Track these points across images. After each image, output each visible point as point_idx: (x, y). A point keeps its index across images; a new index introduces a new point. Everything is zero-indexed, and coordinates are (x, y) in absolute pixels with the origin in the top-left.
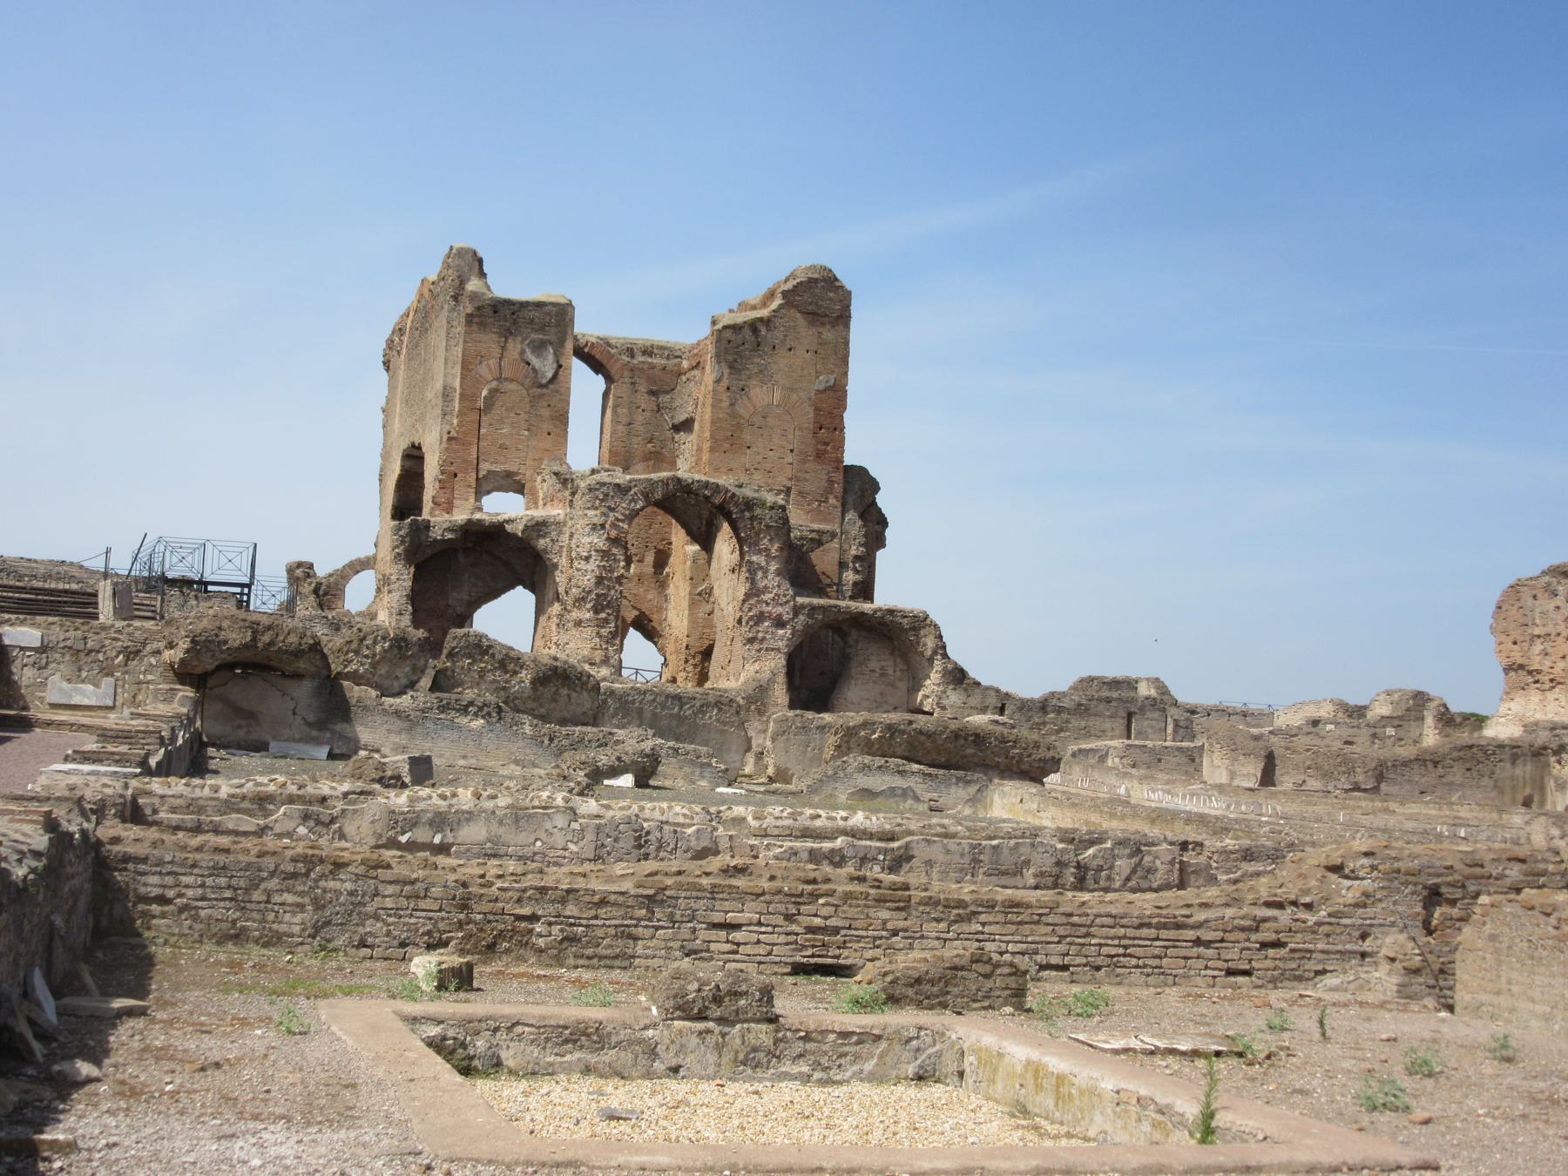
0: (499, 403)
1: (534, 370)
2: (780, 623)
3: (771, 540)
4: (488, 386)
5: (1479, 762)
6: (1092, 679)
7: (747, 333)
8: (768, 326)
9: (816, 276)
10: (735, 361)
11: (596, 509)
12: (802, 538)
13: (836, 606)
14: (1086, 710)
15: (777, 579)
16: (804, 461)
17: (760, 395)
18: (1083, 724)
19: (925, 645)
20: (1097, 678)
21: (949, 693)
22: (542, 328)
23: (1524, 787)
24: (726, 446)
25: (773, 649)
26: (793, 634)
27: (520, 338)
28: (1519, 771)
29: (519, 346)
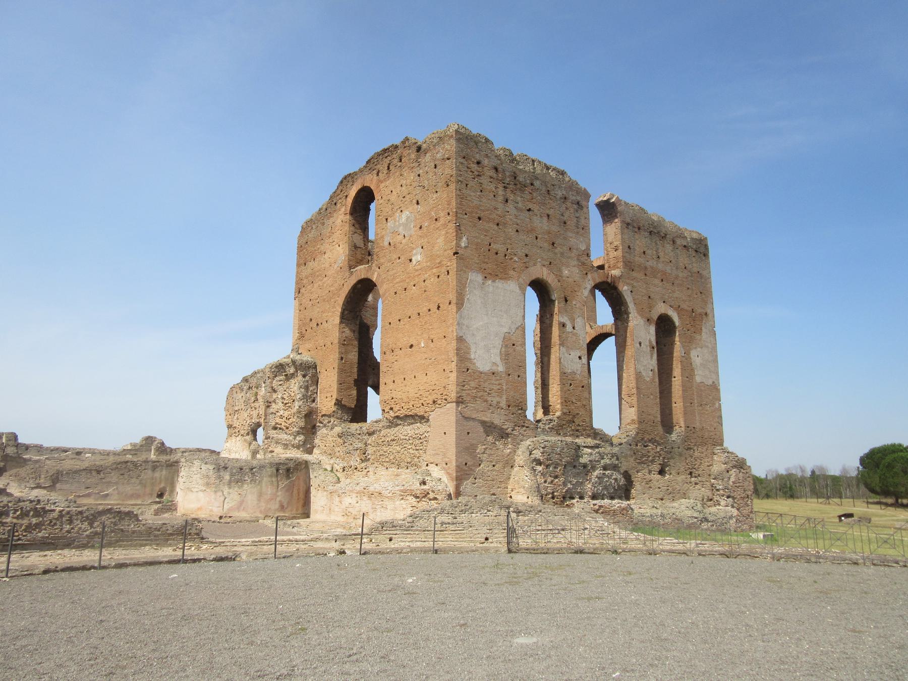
5: (129, 471)
23: (160, 482)
28: (157, 474)
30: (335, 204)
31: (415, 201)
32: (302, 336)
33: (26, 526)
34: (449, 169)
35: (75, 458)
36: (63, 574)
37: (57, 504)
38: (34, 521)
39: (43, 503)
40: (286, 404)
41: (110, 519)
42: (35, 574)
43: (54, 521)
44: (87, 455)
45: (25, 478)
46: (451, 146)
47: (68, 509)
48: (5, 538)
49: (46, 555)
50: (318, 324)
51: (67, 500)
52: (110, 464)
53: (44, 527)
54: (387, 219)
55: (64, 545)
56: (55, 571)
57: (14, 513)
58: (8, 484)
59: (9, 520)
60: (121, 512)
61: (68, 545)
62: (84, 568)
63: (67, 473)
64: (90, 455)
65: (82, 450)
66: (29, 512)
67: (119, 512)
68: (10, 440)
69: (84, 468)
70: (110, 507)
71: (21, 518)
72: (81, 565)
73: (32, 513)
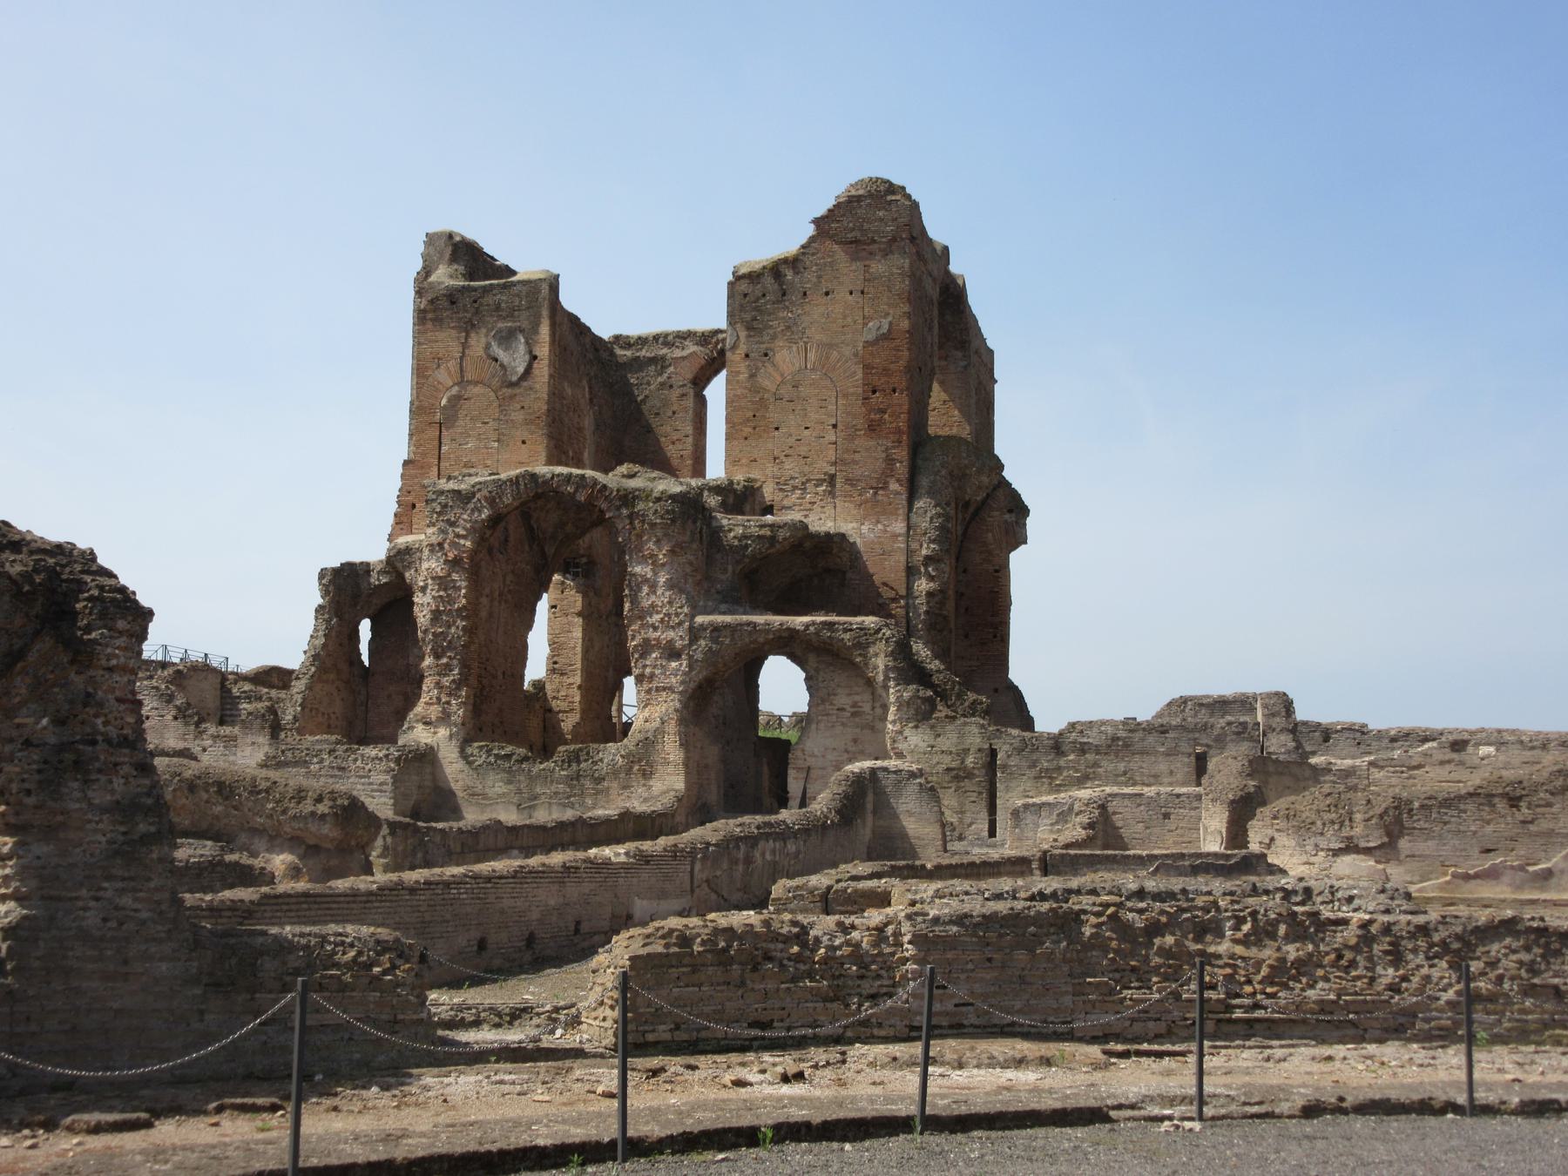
0: (462, 413)
1: (502, 366)
2: (673, 653)
3: (658, 541)
4: (448, 394)
6: (1184, 701)
7: (768, 281)
8: (794, 268)
9: (861, 192)
10: (755, 319)
11: (434, 525)
12: (745, 537)
13: (749, 624)
14: (1126, 746)
15: (668, 593)
16: (851, 438)
17: (787, 358)
18: (1121, 766)
19: (875, 667)
20: (1191, 698)
21: (907, 732)
22: (511, 314)
24: (747, 430)
25: (664, 689)
26: (690, 666)
27: (484, 331)
29: (483, 340)
33: (1271, 966)
35: (1449, 762)
36: (1359, 1124)
37: (1356, 902)
38: (1292, 951)
39: (1319, 899)
41: (1514, 952)
42: (1280, 1117)
43: (1348, 955)
44: (1485, 750)
45: (1312, 823)
47: (1386, 918)
48: (1218, 1000)
49: (1330, 1058)
51: (1383, 891)
52: (1545, 774)
53: (1320, 972)
55: (1386, 1030)
56: (1339, 1109)
57: (1237, 928)
58: (1272, 839)
59: (1223, 947)
60: (1546, 929)
61: (1399, 1027)
62: (1425, 1107)
63: (1422, 806)
64: (1491, 749)
65: (1466, 736)
66: (1274, 924)
67: (1543, 931)
68: (1273, 715)
69: (1471, 790)
70: (1509, 913)
71: (1255, 945)
72: (1416, 1097)
73: (1282, 929)
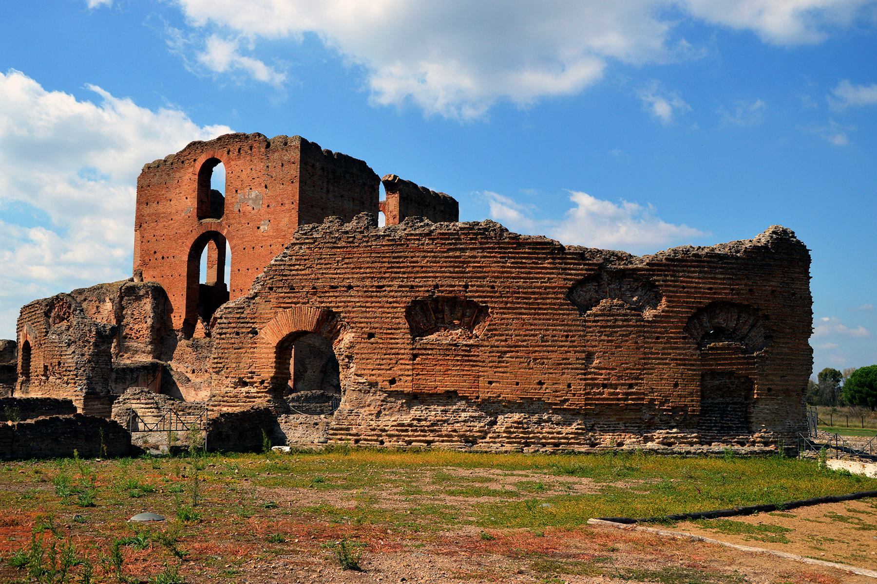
30: (183, 162)
31: (263, 185)
32: (144, 264)
34: (294, 171)
40: (136, 319)
46: (296, 155)
50: (163, 258)
54: (236, 191)
